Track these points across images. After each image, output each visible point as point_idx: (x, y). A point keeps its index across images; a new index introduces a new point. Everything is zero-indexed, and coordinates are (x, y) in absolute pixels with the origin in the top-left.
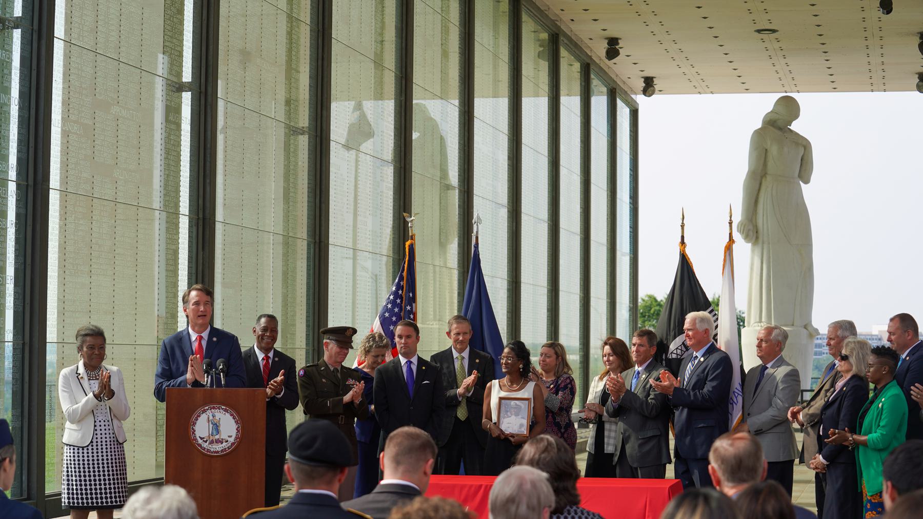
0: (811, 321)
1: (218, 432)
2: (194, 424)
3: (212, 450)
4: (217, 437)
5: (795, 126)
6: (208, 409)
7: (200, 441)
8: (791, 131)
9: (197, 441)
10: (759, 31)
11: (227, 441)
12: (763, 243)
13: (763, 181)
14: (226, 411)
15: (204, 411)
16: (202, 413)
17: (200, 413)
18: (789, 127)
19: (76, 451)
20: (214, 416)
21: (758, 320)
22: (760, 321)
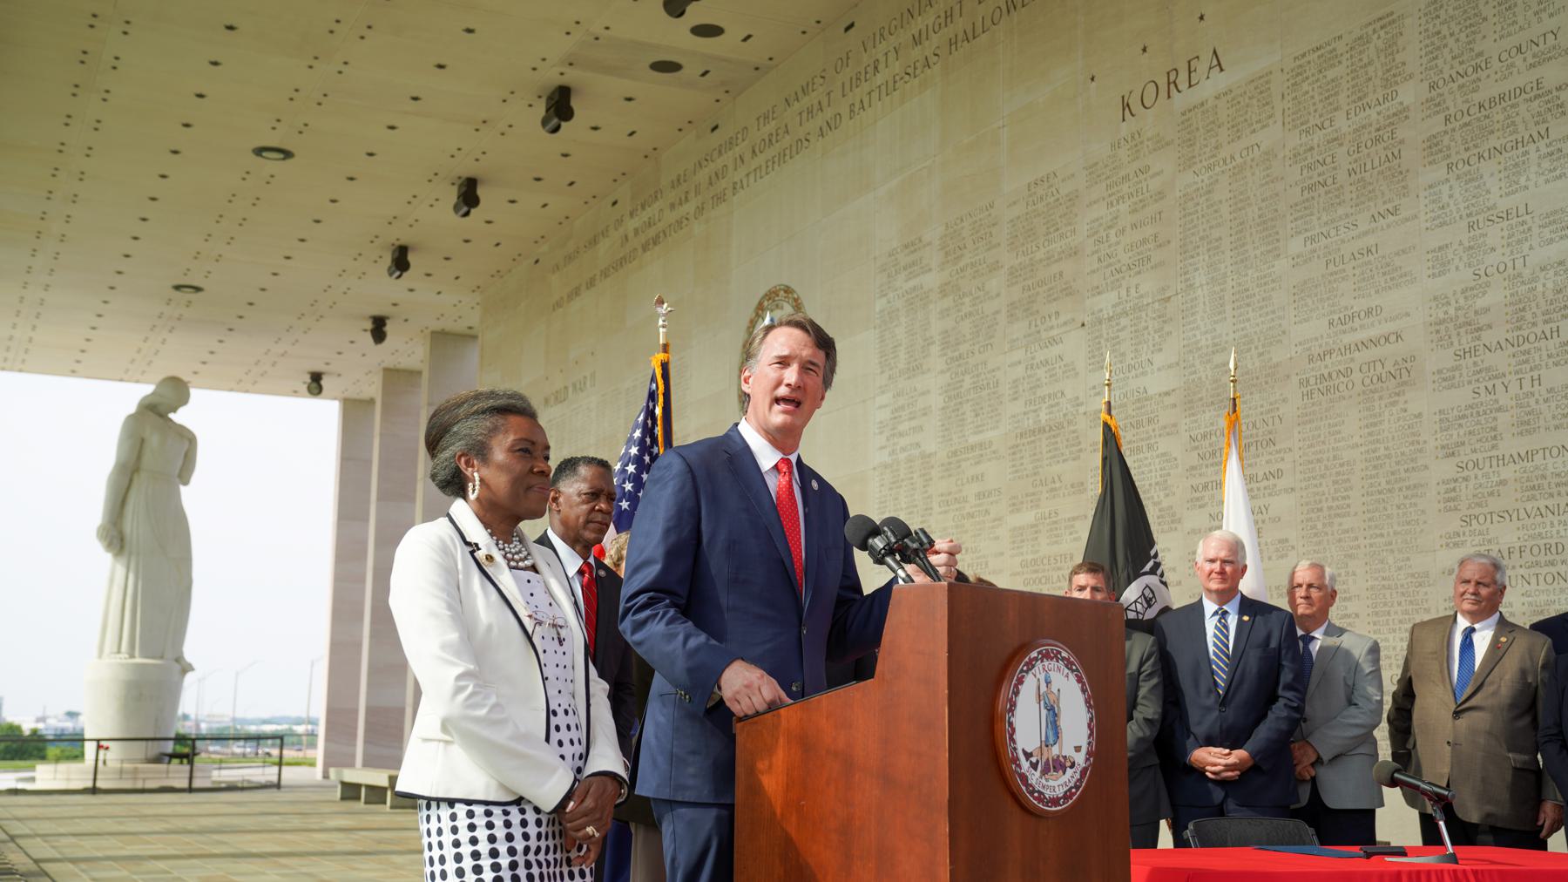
0: (182, 652)
1: (1057, 735)
2: (1014, 705)
3: (1048, 794)
4: (1055, 750)
5: (179, 417)
6: (1036, 659)
7: (1025, 764)
8: (171, 420)
9: (1019, 766)
10: (177, 288)
11: (1072, 766)
12: (130, 554)
13: (136, 477)
14: (1069, 665)
15: (1031, 665)
16: (1027, 672)
17: (1022, 671)
18: (171, 416)
19: (480, 821)
20: (1048, 683)
21: (115, 650)
22: (119, 652)
